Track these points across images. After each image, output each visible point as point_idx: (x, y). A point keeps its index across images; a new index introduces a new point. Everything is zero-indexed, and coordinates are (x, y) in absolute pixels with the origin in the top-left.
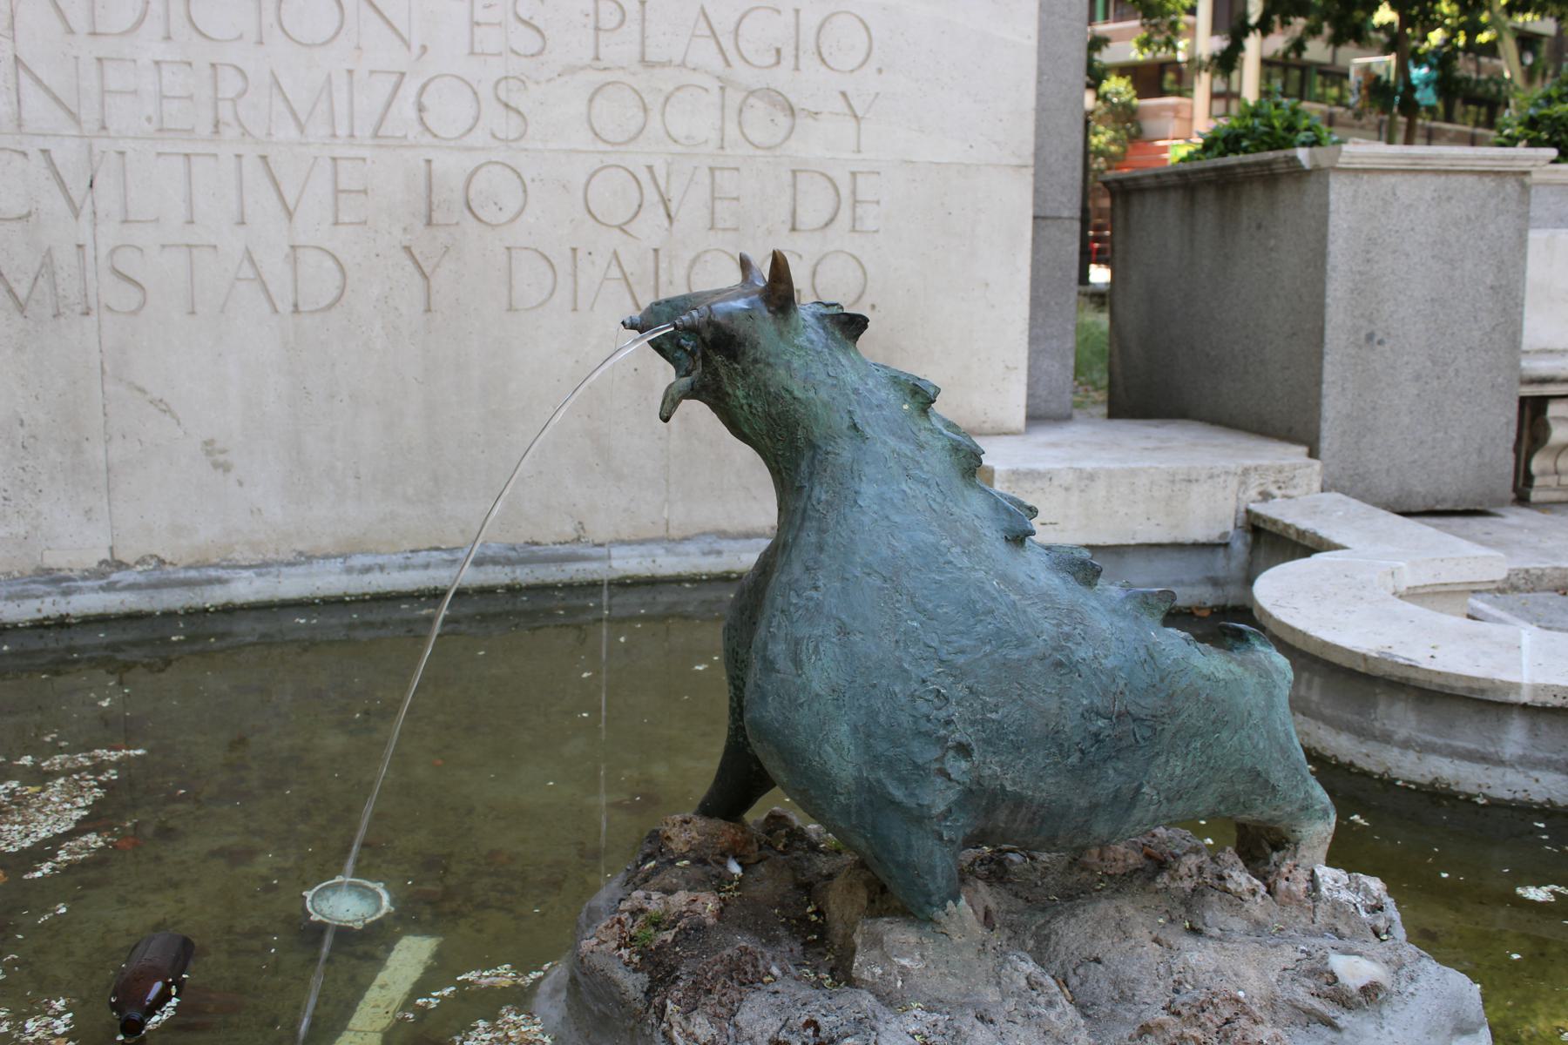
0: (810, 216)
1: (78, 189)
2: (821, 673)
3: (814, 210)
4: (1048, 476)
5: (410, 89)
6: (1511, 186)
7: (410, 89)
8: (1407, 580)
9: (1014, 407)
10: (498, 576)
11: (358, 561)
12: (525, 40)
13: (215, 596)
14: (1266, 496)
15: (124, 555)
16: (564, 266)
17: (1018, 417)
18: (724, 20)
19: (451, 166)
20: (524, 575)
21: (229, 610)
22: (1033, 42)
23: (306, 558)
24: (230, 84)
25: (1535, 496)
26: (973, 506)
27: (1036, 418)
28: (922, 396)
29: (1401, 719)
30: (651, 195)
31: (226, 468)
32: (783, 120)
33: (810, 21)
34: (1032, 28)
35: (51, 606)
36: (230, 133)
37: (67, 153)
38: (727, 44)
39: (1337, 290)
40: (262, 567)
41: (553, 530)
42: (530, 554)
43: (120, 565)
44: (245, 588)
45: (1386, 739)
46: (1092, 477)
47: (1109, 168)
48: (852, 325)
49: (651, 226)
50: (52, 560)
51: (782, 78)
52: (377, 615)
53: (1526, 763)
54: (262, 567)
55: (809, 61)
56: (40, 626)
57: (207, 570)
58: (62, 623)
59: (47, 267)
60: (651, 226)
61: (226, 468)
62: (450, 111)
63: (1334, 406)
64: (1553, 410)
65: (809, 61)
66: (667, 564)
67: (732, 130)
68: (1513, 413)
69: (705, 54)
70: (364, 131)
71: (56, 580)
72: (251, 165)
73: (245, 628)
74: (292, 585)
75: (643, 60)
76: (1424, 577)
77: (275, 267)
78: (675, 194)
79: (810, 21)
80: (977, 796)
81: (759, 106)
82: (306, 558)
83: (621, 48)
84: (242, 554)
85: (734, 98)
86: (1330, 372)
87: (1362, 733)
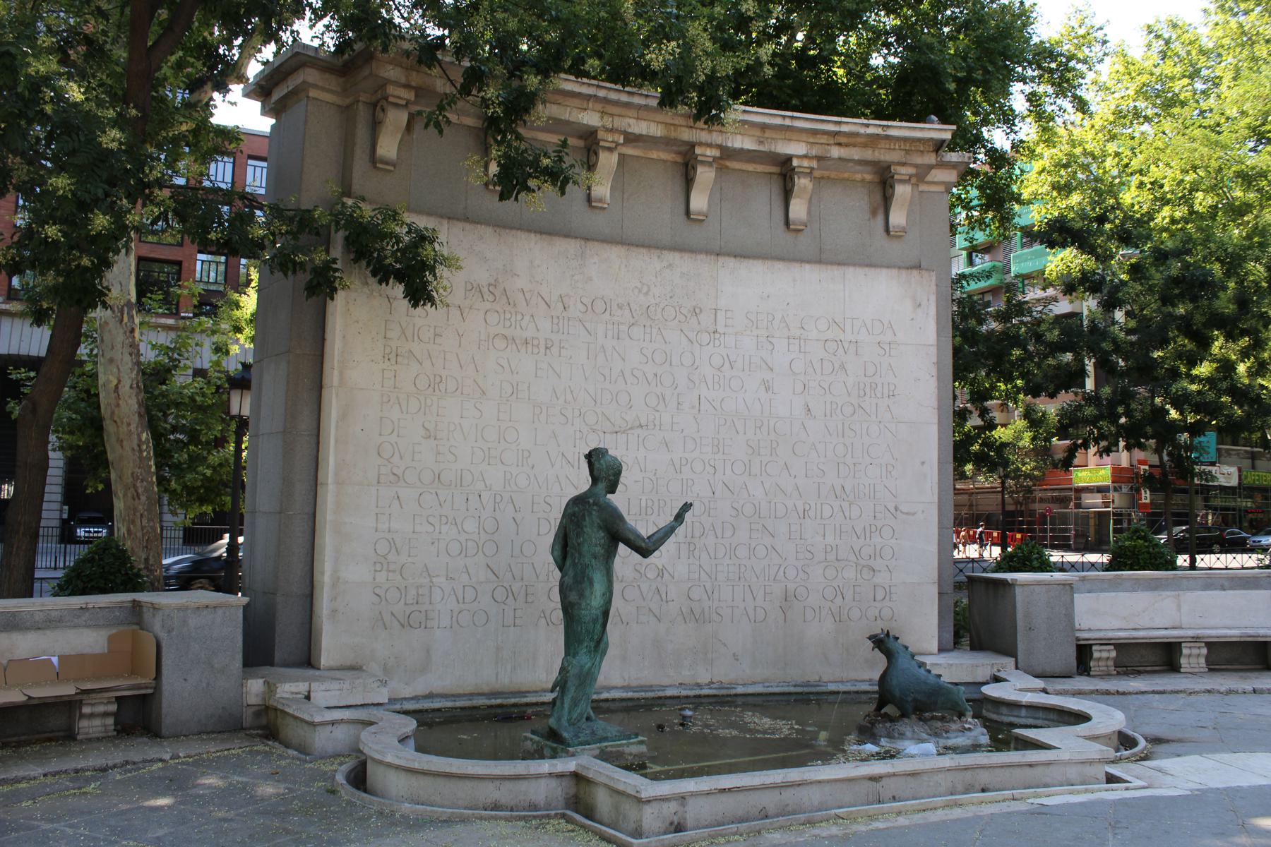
0: (879, 597)
1: (710, 593)
2: (894, 682)
3: (880, 596)
4: (940, 665)
5: (782, 569)
6: (1067, 587)
7: (782, 569)
8: (1019, 687)
9: (934, 646)
10: (799, 690)
11: (766, 684)
12: (809, 555)
13: (733, 692)
14: (999, 671)
15: (714, 680)
16: (817, 611)
17: (936, 650)
18: (856, 549)
19: (791, 586)
20: (806, 690)
21: (736, 695)
22: (936, 551)
23: (754, 683)
24: (743, 569)
25: (1092, 673)
26: (914, 662)
27: (941, 650)
28: (907, 648)
29: (1004, 710)
30: (839, 593)
31: (737, 660)
32: (872, 573)
33: (878, 548)
34: (936, 547)
35: (698, 692)
36: (742, 580)
37: (708, 586)
38: (857, 554)
39: (1020, 616)
40: (744, 685)
41: (813, 678)
42: (807, 684)
43: (713, 683)
44: (740, 690)
45: (1002, 714)
46: (951, 665)
47: (1034, 485)
48: (897, 638)
49: (839, 600)
50: (699, 681)
51: (871, 563)
52: (770, 698)
53: (1026, 717)
54: (744, 685)
55: (878, 558)
56: (695, 697)
57: (732, 685)
58: (699, 696)
59: (703, 611)
60: (839, 600)
61: (737, 660)
62: (791, 573)
63: (1021, 647)
64: (1094, 648)
65: (878, 558)
66: (842, 688)
67: (859, 576)
68: (1074, 648)
69: (852, 557)
70: (771, 579)
71: (699, 686)
72: (747, 588)
73: (740, 701)
74: (751, 690)
75: (837, 560)
76: (1023, 686)
77: (751, 612)
78: (844, 592)
79: (878, 548)
80: (915, 700)
81: (865, 571)
82: (754, 683)
83: (831, 557)
84: (740, 682)
85: (859, 568)
86: (1019, 638)
87: (998, 714)
